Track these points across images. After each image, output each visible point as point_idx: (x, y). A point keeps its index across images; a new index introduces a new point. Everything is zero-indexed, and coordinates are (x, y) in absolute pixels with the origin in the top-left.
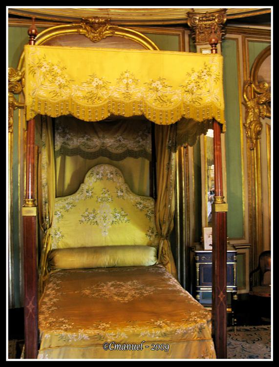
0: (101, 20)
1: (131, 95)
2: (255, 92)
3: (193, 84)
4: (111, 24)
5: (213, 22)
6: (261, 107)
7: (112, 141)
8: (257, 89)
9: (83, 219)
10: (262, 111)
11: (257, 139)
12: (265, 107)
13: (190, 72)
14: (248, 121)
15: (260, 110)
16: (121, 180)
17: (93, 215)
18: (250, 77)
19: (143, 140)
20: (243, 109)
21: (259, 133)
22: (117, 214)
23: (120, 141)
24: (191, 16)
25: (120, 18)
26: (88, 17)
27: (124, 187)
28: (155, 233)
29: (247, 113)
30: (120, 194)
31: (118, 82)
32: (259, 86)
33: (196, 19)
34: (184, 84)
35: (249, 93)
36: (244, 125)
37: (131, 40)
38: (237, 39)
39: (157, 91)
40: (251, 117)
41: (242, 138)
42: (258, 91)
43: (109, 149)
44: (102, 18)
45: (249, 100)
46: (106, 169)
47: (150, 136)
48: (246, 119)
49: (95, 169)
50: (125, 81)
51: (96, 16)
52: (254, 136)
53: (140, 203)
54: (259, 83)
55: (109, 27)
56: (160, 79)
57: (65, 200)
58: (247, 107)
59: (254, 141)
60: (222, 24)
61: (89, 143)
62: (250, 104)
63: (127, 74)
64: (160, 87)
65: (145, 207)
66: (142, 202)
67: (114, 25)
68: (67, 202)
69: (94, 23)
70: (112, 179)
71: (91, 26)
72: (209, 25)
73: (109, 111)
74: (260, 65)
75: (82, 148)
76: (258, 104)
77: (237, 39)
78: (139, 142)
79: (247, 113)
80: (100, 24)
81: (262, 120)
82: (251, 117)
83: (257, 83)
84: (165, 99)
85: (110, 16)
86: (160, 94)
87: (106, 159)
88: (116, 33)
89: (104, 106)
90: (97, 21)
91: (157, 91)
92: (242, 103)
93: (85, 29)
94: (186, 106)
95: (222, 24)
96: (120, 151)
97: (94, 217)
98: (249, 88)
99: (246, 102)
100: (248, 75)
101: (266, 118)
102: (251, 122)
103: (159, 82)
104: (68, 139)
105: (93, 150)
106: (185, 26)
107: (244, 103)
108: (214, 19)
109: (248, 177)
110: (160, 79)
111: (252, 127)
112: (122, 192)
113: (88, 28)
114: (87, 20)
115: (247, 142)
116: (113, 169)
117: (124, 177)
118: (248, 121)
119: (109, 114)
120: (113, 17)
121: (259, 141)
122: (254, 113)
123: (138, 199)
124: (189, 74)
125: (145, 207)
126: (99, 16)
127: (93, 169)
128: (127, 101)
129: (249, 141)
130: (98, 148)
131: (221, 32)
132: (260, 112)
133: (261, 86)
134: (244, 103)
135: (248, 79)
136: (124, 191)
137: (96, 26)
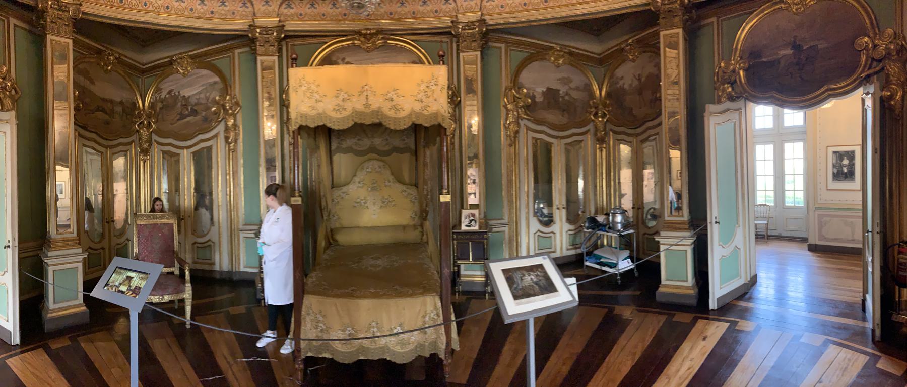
0: (372, 31)
1: (370, 105)
2: (515, 96)
3: (422, 94)
4: (384, 34)
5: (474, 31)
6: (520, 110)
7: (381, 140)
8: (517, 93)
10: (520, 113)
11: (515, 137)
12: (523, 110)
13: (420, 82)
14: (508, 122)
15: (518, 112)
16: (388, 172)
17: (364, 201)
18: (511, 83)
19: (408, 138)
20: (503, 111)
21: (517, 132)
22: (384, 200)
23: (387, 140)
24: (455, 24)
25: (391, 27)
26: (361, 29)
27: (391, 178)
28: (418, 216)
29: (508, 114)
30: (387, 183)
31: (359, 95)
32: (519, 91)
33: (459, 28)
34: (415, 94)
35: (510, 97)
36: (504, 125)
37: (402, 48)
38: (500, 48)
39: (392, 101)
40: (511, 119)
41: (502, 136)
42: (517, 95)
44: (373, 29)
45: (509, 104)
46: (377, 164)
47: (414, 135)
48: (506, 120)
49: (366, 164)
50: (365, 93)
51: (367, 27)
52: (513, 135)
53: (405, 191)
54: (519, 88)
55: (381, 36)
56: (394, 90)
57: (341, 190)
58: (508, 110)
59: (513, 139)
60: (481, 33)
61: (360, 143)
62: (509, 107)
63: (366, 87)
64: (394, 97)
65: (409, 194)
66: (406, 190)
67: (386, 34)
68: (342, 191)
69: (366, 34)
70: (380, 171)
71: (364, 37)
72: (471, 33)
73: (353, 120)
74: (520, 73)
75: (354, 147)
76: (517, 106)
77: (500, 48)
78: (404, 140)
79: (508, 114)
80: (372, 35)
81: (520, 121)
82: (511, 119)
83: (517, 88)
84: (399, 107)
85: (381, 27)
86: (394, 103)
87: (374, 155)
88: (389, 42)
89: (349, 116)
90: (368, 32)
91: (392, 101)
92: (504, 106)
93: (359, 40)
94: (418, 114)
95: (481, 33)
96: (387, 148)
98: (510, 92)
99: (507, 105)
100: (510, 81)
101: (524, 120)
102: (510, 123)
103: (393, 93)
104: (342, 140)
105: (364, 149)
106: (449, 33)
107: (505, 106)
108: (475, 28)
109: (508, 168)
110: (394, 90)
111: (511, 127)
112: (389, 182)
114: (360, 32)
115: (507, 140)
116: (381, 164)
117: (391, 170)
118: (508, 122)
119: (353, 123)
120: (384, 27)
121: (517, 139)
122: (513, 114)
123: (404, 188)
124: (419, 85)
125: (409, 194)
126: (370, 27)
127: (363, 164)
128: (367, 111)
129: (509, 139)
130: (368, 146)
131: (481, 41)
132: (518, 114)
133: (521, 91)
134: (505, 106)
135: (510, 84)
136: (391, 181)
137: (368, 37)
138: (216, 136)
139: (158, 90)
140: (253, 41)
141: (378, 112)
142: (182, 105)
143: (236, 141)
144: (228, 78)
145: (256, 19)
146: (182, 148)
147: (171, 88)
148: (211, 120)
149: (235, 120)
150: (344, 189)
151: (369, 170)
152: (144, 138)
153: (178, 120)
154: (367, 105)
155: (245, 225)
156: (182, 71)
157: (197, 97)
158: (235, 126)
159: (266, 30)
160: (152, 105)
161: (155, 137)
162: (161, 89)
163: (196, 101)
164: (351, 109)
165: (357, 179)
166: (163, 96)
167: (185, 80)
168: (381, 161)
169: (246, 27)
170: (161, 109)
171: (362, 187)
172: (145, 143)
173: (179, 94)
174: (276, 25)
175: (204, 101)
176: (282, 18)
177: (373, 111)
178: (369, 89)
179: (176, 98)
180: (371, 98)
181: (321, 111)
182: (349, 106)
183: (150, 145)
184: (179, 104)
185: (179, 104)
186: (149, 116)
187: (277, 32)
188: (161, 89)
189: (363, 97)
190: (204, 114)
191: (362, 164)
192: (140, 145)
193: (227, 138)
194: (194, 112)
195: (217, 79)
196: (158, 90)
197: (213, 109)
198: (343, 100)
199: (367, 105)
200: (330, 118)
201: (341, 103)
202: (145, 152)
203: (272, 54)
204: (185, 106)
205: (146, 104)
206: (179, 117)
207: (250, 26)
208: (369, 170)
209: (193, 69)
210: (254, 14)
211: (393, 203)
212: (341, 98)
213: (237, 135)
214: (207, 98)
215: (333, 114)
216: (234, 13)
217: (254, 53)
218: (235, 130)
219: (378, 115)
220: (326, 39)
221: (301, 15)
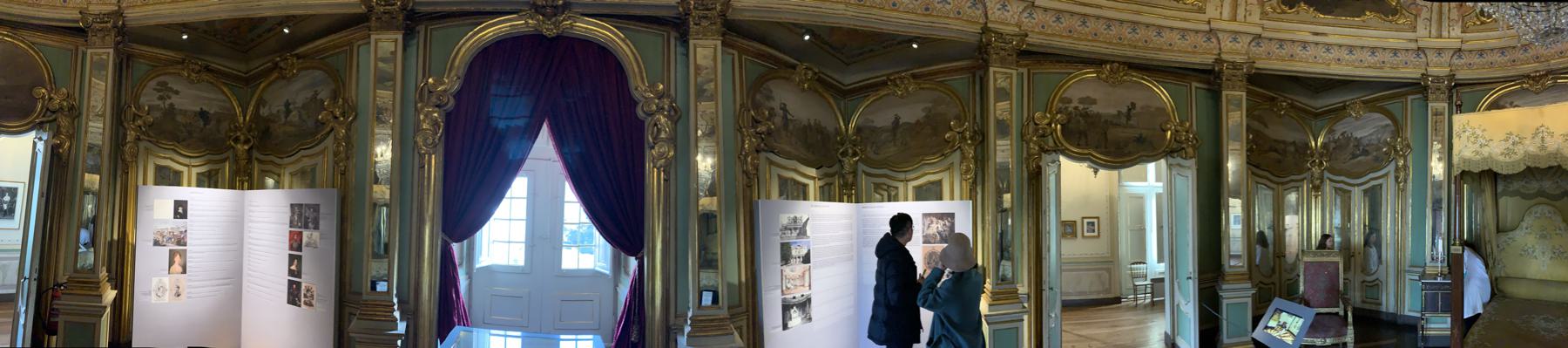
9: (1523, 253)
16: (1559, 219)
23: (1557, 182)
30: (1558, 232)
43: (1547, 191)
46: (1546, 209)
49: (1534, 209)
61: (1527, 185)
70: (1550, 218)
75: (1522, 190)
87: (1543, 199)
90: (1538, 74)
93: (1528, 83)
97: (1533, 252)
104: (1509, 183)
105: (1532, 192)
113: (1531, 82)
116: (1550, 208)
130: (1536, 190)
136: (1562, 228)
138: (1386, 175)
139: (1331, 131)
140: (1426, 88)
141: (1556, 154)
142: (1354, 146)
143: (1405, 181)
144: (1400, 120)
145: (1428, 69)
146: (1353, 185)
147: (1344, 130)
148: (1383, 160)
149: (1405, 161)
150: (1511, 234)
151: (1538, 215)
152: (1316, 175)
153: (1351, 159)
154: (1543, 148)
155: (1411, 266)
156: (1354, 115)
157: (1369, 138)
158: (1405, 166)
159: (1437, 79)
160: (1324, 145)
161: (1327, 174)
162: (1334, 131)
163: (1367, 142)
164: (1522, 152)
165: (1524, 224)
166: (1336, 138)
167: (1359, 123)
168: (1553, 206)
169: (1419, 76)
170: (1334, 149)
171: (1530, 233)
172: (1317, 179)
173: (1352, 136)
174: (1447, 74)
175: (1375, 142)
176: (1453, 68)
177: (1549, 154)
178: (1545, 130)
179: (1349, 139)
180: (1548, 139)
181: (1486, 155)
182: (1520, 150)
183: (1322, 182)
184: (1352, 144)
185: (1352, 144)
186: (1321, 155)
187: (1448, 80)
188: (1334, 131)
189: (1538, 140)
190: (1375, 154)
191: (1529, 208)
192: (1312, 182)
193: (1397, 178)
194: (1365, 153)
195: (1389, 122)
196: (1331, 131)
197: (1384, 150)
198: (1513, 144)
199: (1543, 148)
200: (1497, 162)
201: (1511, 147)
202: (1317, 188)
203: (1443, 101)
204: (1357, 146)
205: (1319, 144)
206: (1351, 156)
207: (1423, 75)
208: (1538, 215)
209: (1365, 113)
210: (1428, 64)
211: (1565, 255)
212: (1511, 141)
213: (1407, 175)
214: (1379, 140)
215: (1501, 158)
216: (1406, 63)
217: (1426, 99)
218: (1405, 170)
219: (1556, 158)
220: (1494, 86)
221: (1470, 64)
